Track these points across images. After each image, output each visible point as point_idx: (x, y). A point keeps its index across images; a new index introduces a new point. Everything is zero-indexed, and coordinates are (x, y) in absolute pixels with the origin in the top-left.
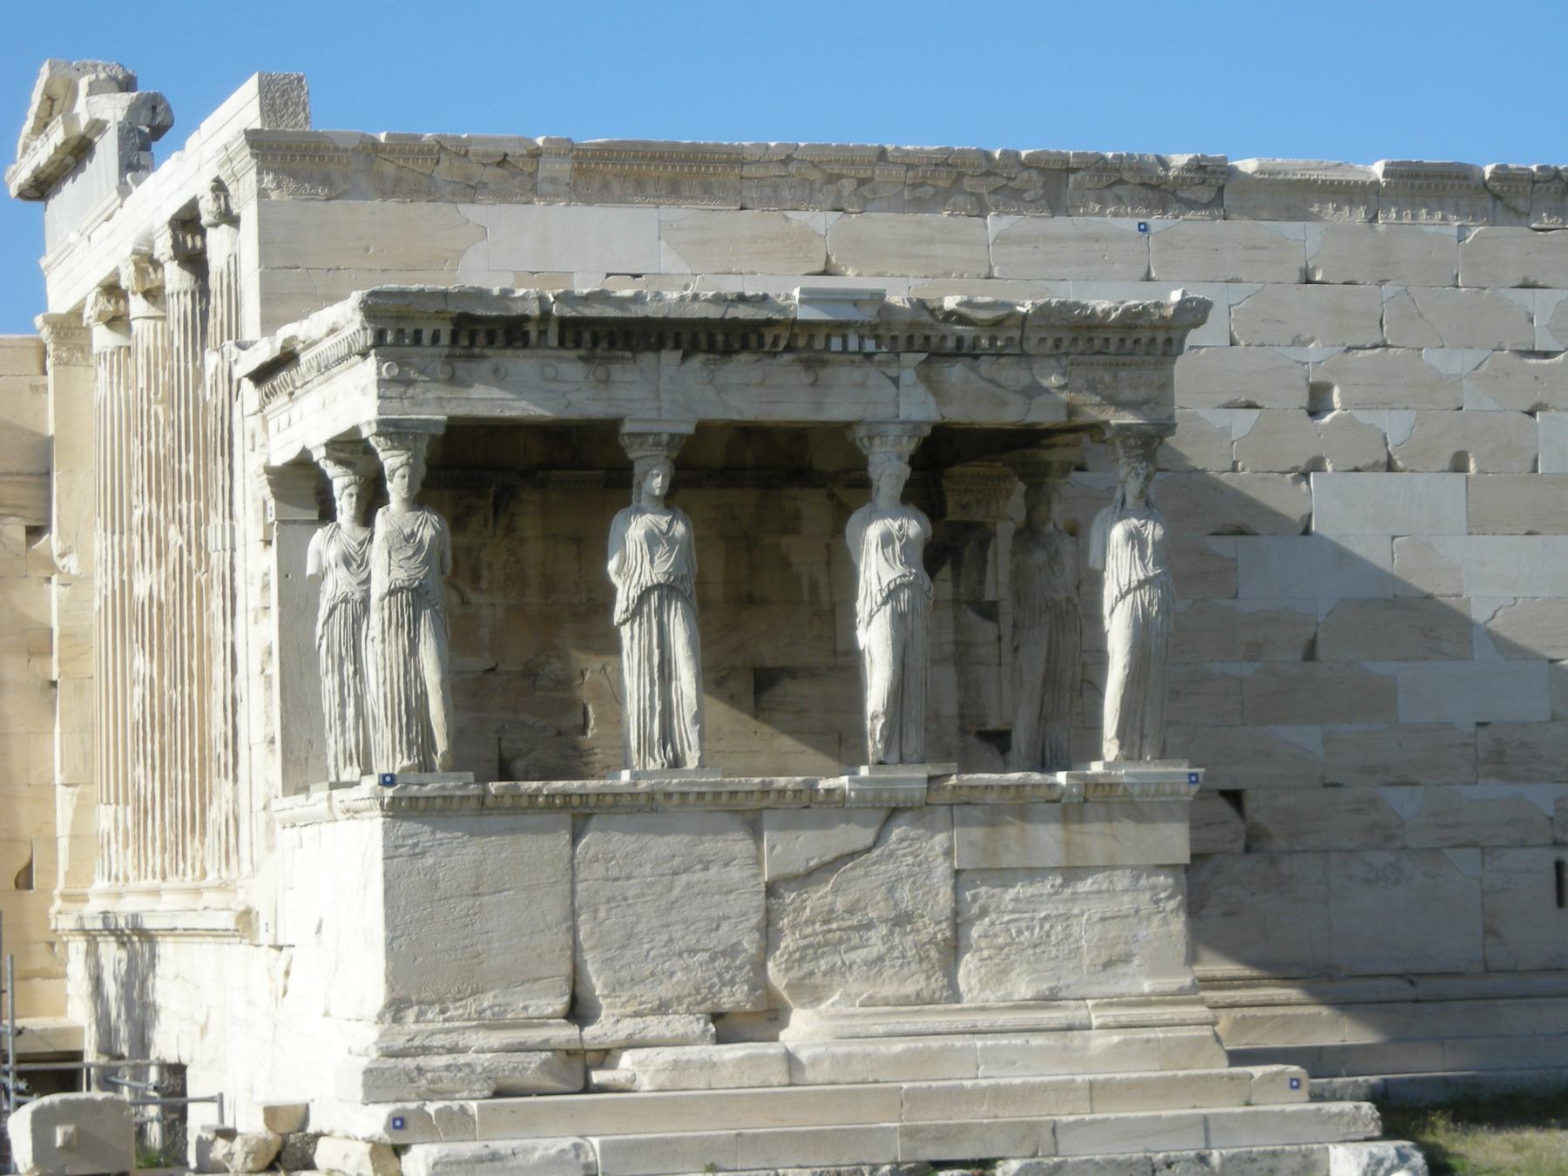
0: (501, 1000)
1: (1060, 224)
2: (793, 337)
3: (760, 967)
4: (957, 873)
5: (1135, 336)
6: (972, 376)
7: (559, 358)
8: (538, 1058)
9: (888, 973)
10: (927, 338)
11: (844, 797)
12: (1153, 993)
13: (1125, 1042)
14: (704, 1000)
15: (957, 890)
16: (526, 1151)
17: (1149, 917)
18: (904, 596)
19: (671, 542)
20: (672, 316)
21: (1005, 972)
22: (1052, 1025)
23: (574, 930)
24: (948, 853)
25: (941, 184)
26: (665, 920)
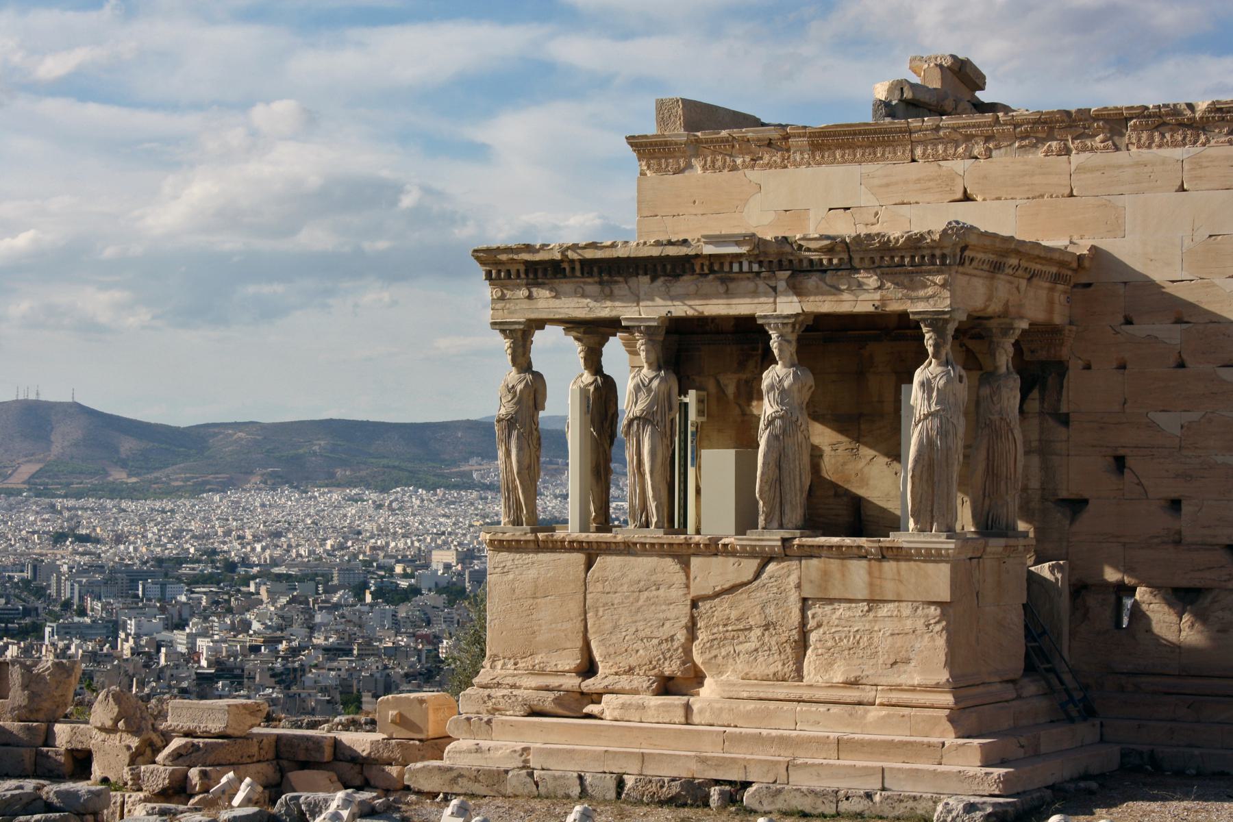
0: (545, 659)
1: (1122, 156)
2: (711, 265)
3: (688, 652)
4: (804, 600)
5: (920, 253)
6: (821, 284)
7: (585, 283)
8: (551, 696)
9: (760, 659)
10: (791, 261)
11: (733, 548)
12: (919, 685)
13: (888, 716)
14: (654, 668)
15: (803, 611)
16: (497, 749)
17: (922, 635)
18: (778, 422)
19: (649, 390)
20: (632, 255)
21: (831, 664)
22: (848, 700)
23: (585, 620)
24: (798, 586)
25: (1040, 135)
26: (634, 618)
